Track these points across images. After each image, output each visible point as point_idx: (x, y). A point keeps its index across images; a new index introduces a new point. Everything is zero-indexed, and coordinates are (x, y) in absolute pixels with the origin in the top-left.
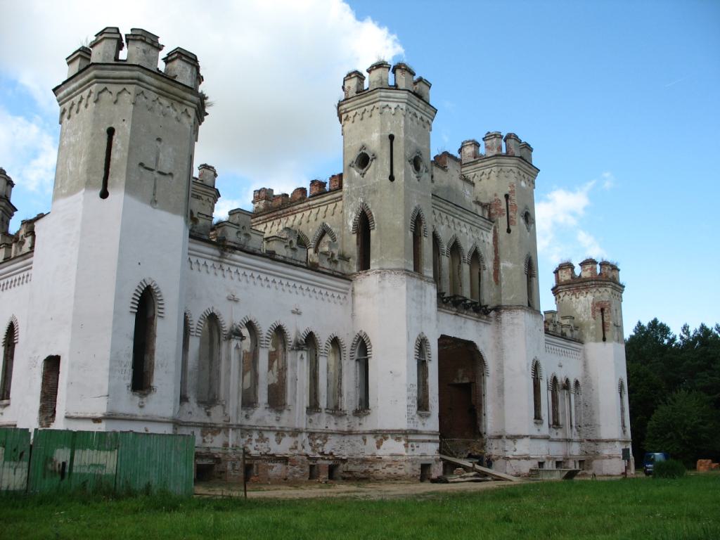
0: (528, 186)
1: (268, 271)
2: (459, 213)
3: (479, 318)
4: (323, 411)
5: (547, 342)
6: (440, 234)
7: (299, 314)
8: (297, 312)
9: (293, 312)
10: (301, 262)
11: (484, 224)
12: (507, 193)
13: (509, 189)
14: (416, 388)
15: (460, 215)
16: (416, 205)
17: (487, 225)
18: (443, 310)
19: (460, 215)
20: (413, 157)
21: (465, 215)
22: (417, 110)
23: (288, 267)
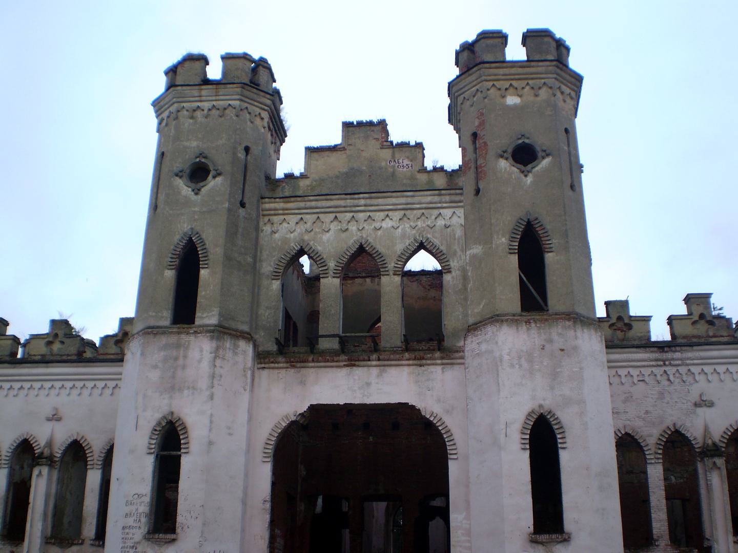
0: (531, 98)
1: (10, 378)
2: (362, 202)
3: (422, 358)
4: (88, 542)
5: (612, 365)
6: (319, 248)
7: (59, 419)
8: (55, 417)
9: (49, 420)
10: (68, 355)
11: (436, 199)
12: (474, 130)
13: (477, 123)
14: (147, 499)
15: (365, 206)
16: (186, 227)
17: (447, 198)
18: (311, 364)
19: (365, 206)
20: (187, 167)
21: (380, 201)
22: (201, 101)
23: (37, 367)
